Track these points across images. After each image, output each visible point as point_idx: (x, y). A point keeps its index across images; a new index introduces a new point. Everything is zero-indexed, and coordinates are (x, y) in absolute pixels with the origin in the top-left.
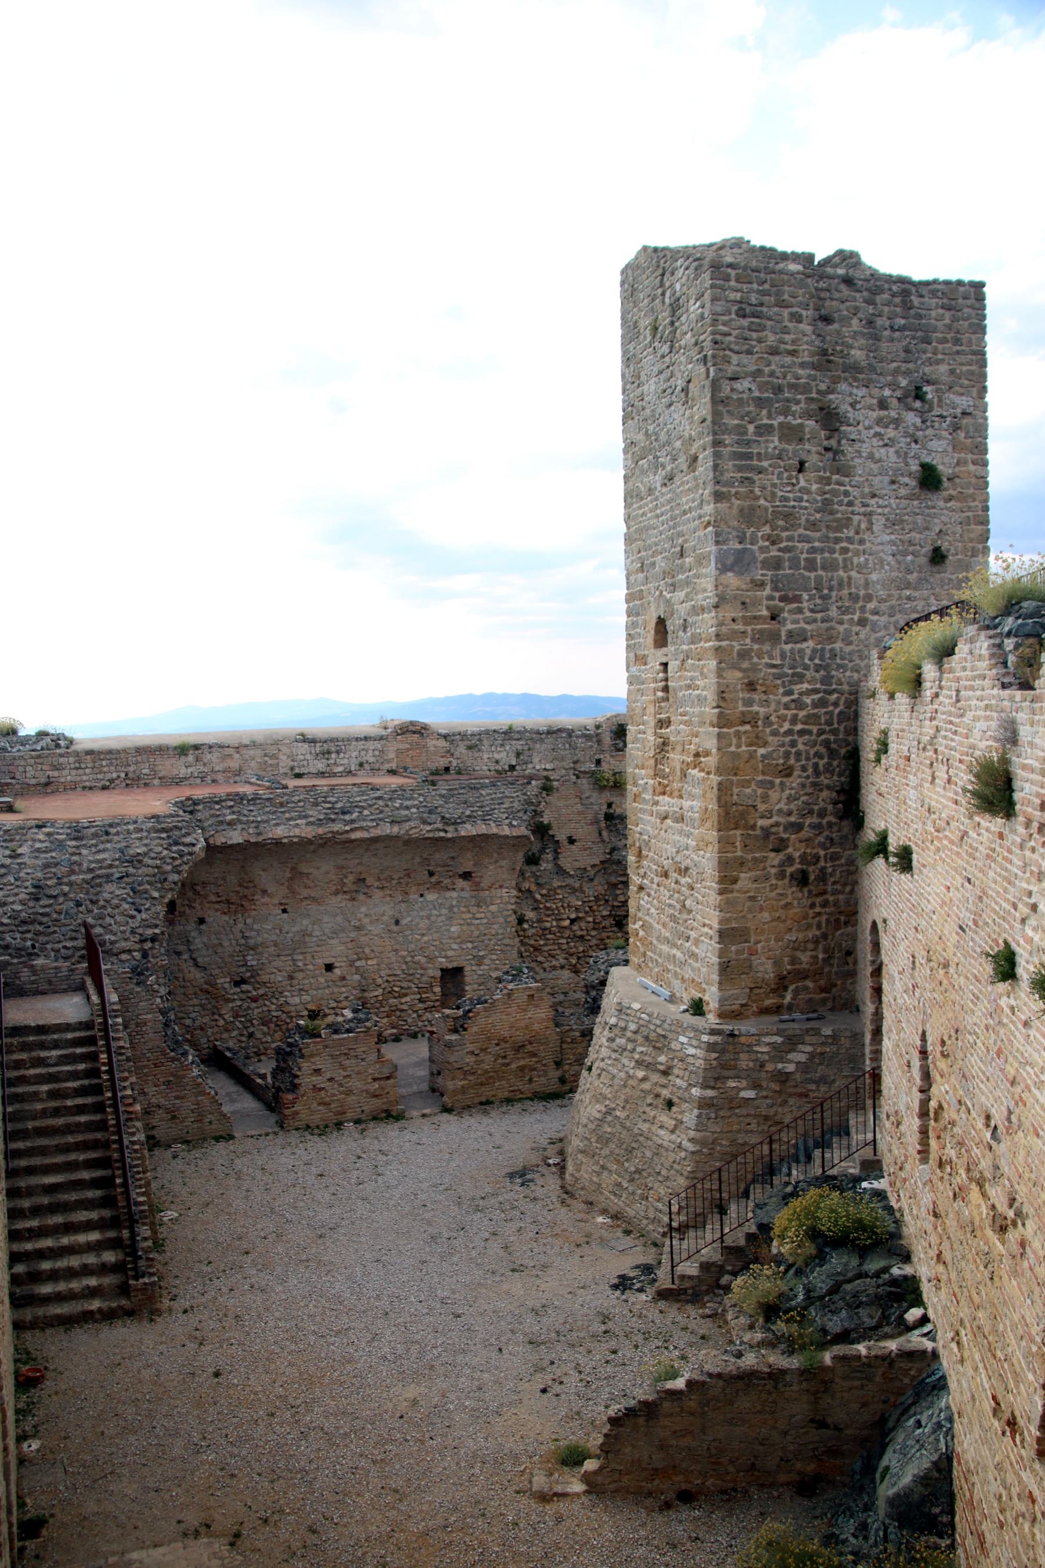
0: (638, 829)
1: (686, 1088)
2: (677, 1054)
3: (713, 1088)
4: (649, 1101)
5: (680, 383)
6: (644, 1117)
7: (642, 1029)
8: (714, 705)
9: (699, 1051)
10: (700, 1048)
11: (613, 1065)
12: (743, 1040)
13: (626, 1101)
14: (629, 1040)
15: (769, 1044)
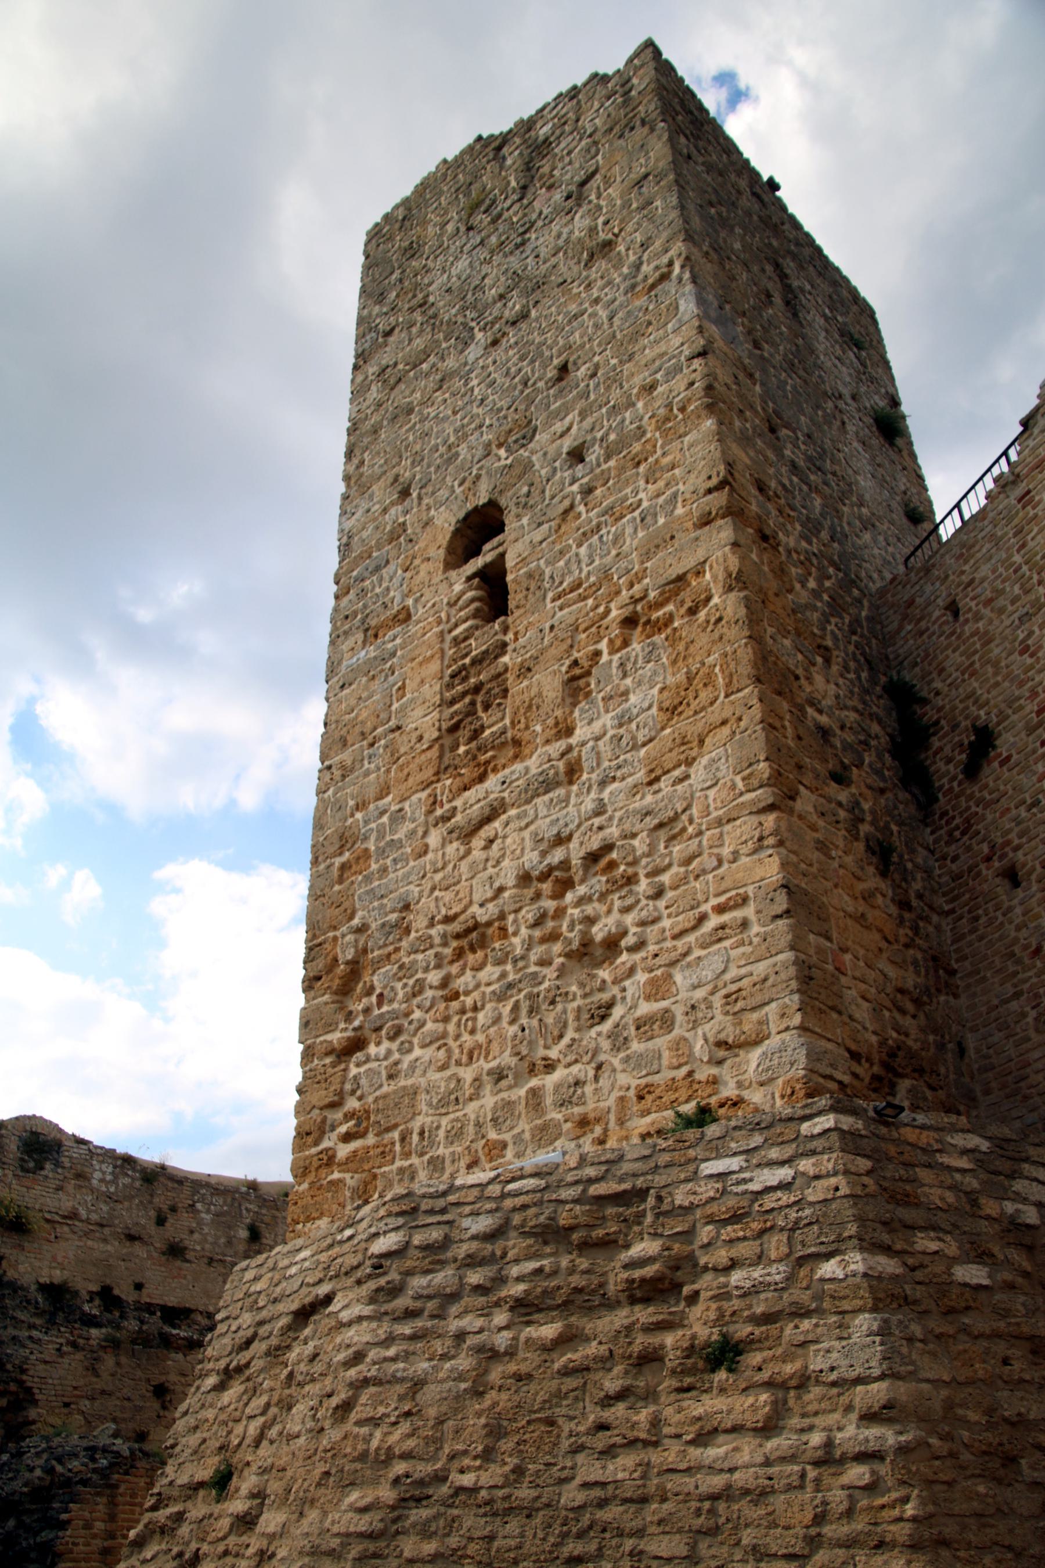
0: (356, 921)
1: (790, 1278)
2: (713, 1208)
3: (887, 1250)
4: (611, 1384)
5: (558, 196)
6: (602, 1440)
7: (517, 1219)
8: (715, 481)
9: (806, 1165)
10: (813, 1153)
11: (406, 1356)
12: (909, 1134)
13: (495, 1432)
14: (472, 1261)
15: (965, 1152)
